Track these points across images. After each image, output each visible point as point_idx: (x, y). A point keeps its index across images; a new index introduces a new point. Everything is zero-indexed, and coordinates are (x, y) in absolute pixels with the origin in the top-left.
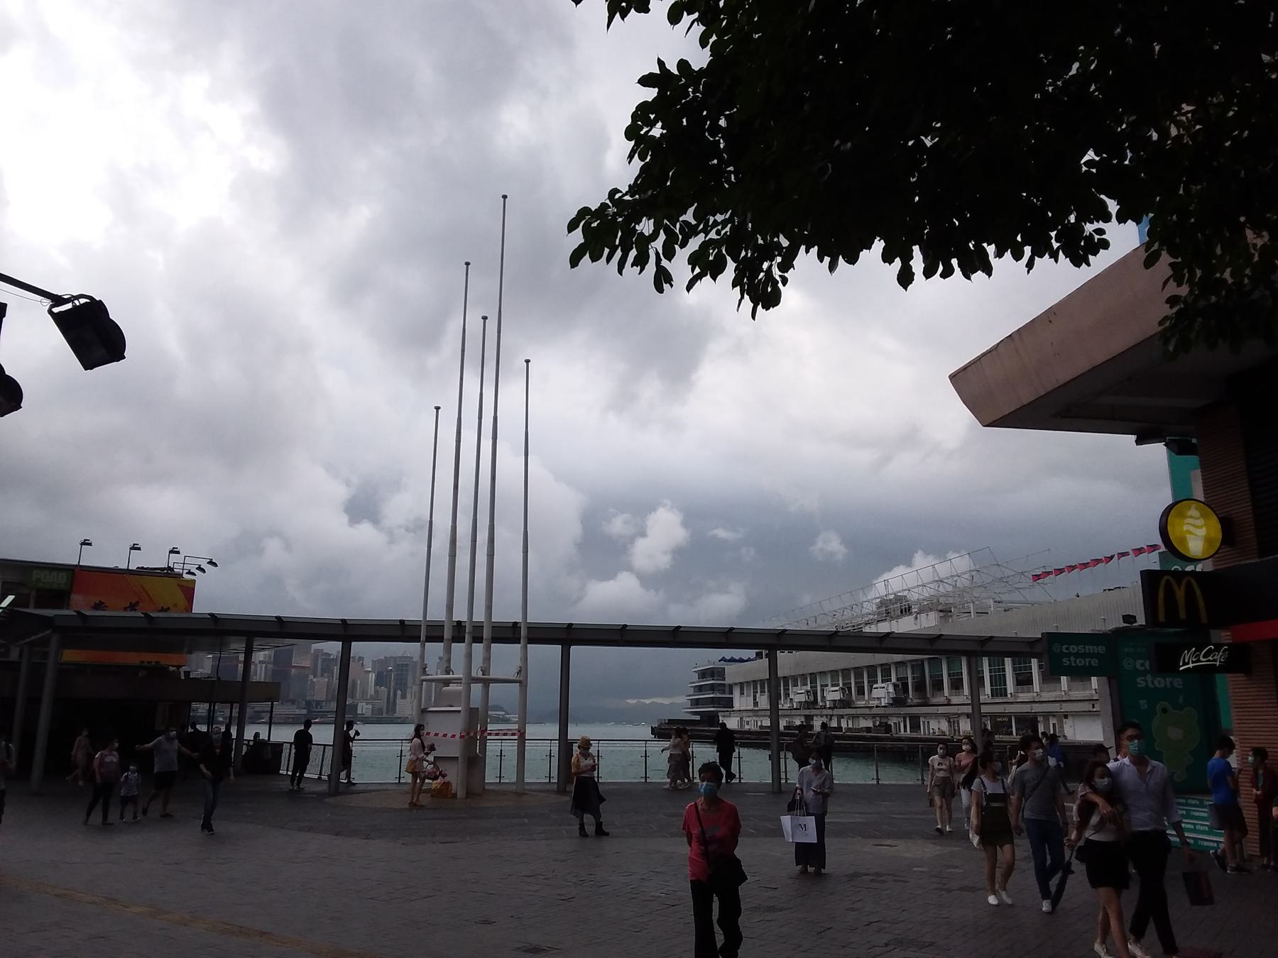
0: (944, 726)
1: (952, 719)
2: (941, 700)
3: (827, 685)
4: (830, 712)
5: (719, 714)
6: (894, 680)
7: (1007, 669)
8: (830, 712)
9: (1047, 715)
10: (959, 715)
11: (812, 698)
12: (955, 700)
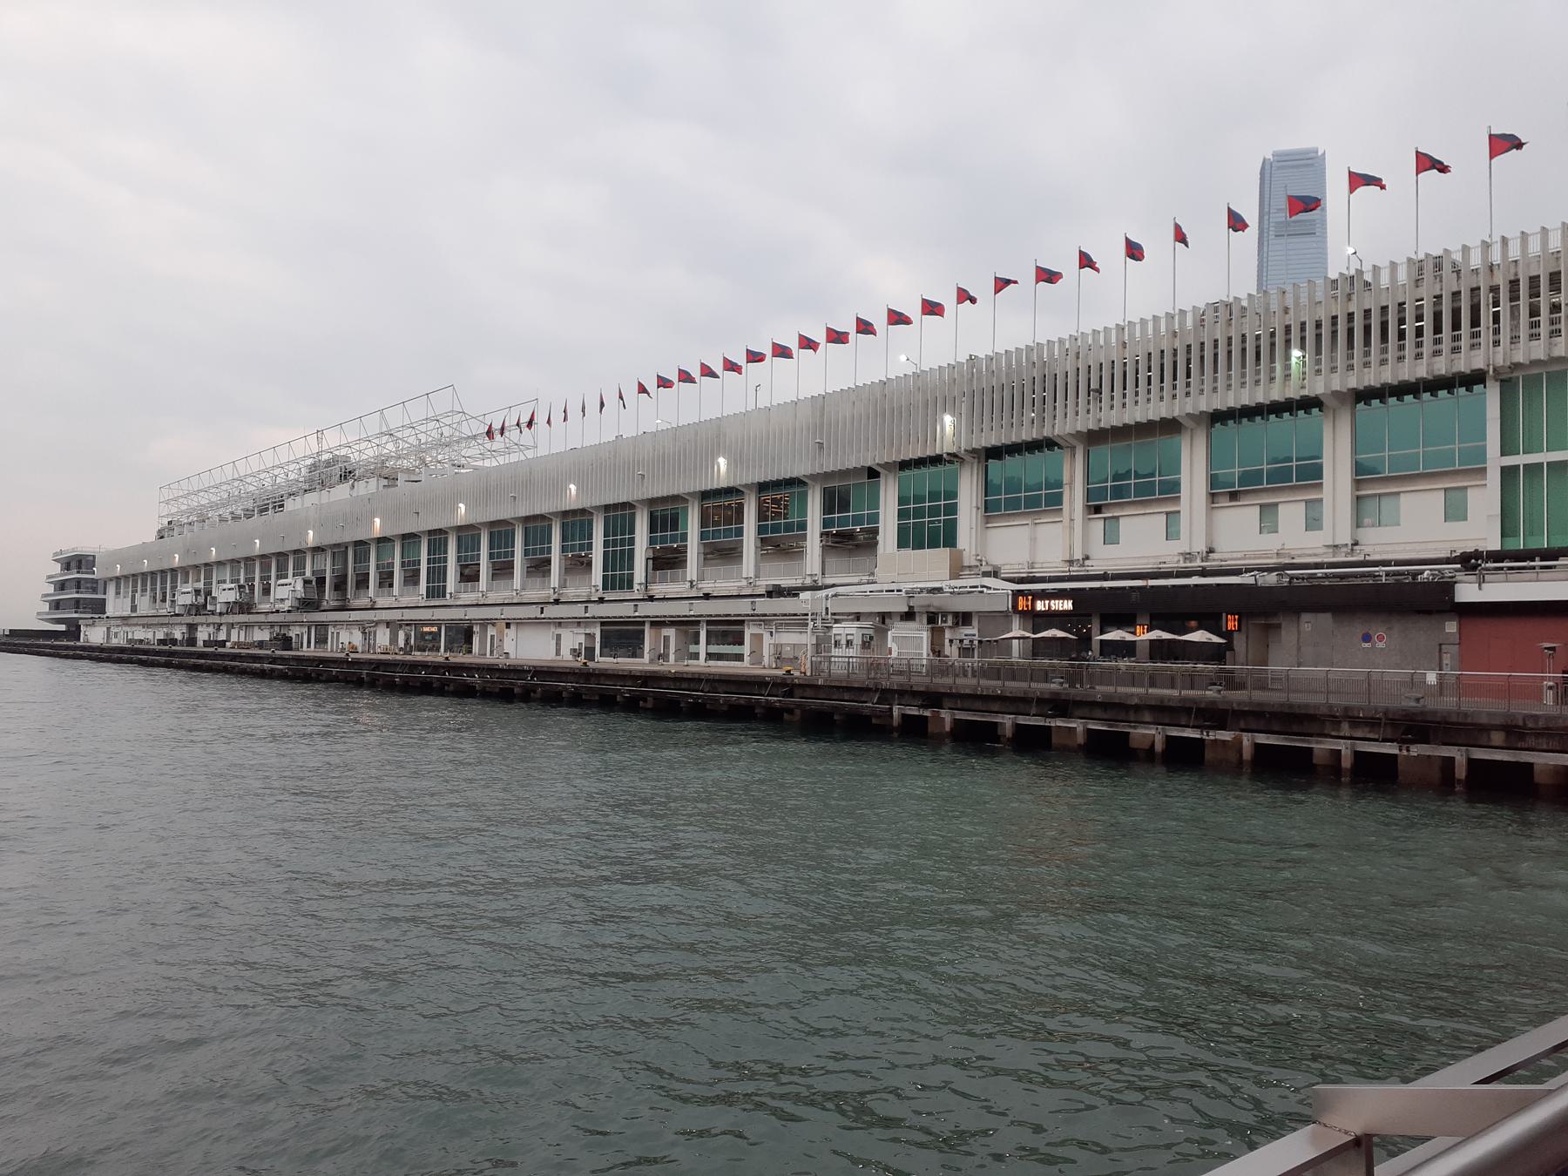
0: (356, 638)
1: (367, 629)
2: (363, 601)
3: (224, 582)
4: (216, 619)
5: (80, 622)
6: (308, 574)
7: (449, 559)
8: (216, 619)
9: (485, 623)
10: (377, 623)
11: (201, 600)
12: (382, 602)
